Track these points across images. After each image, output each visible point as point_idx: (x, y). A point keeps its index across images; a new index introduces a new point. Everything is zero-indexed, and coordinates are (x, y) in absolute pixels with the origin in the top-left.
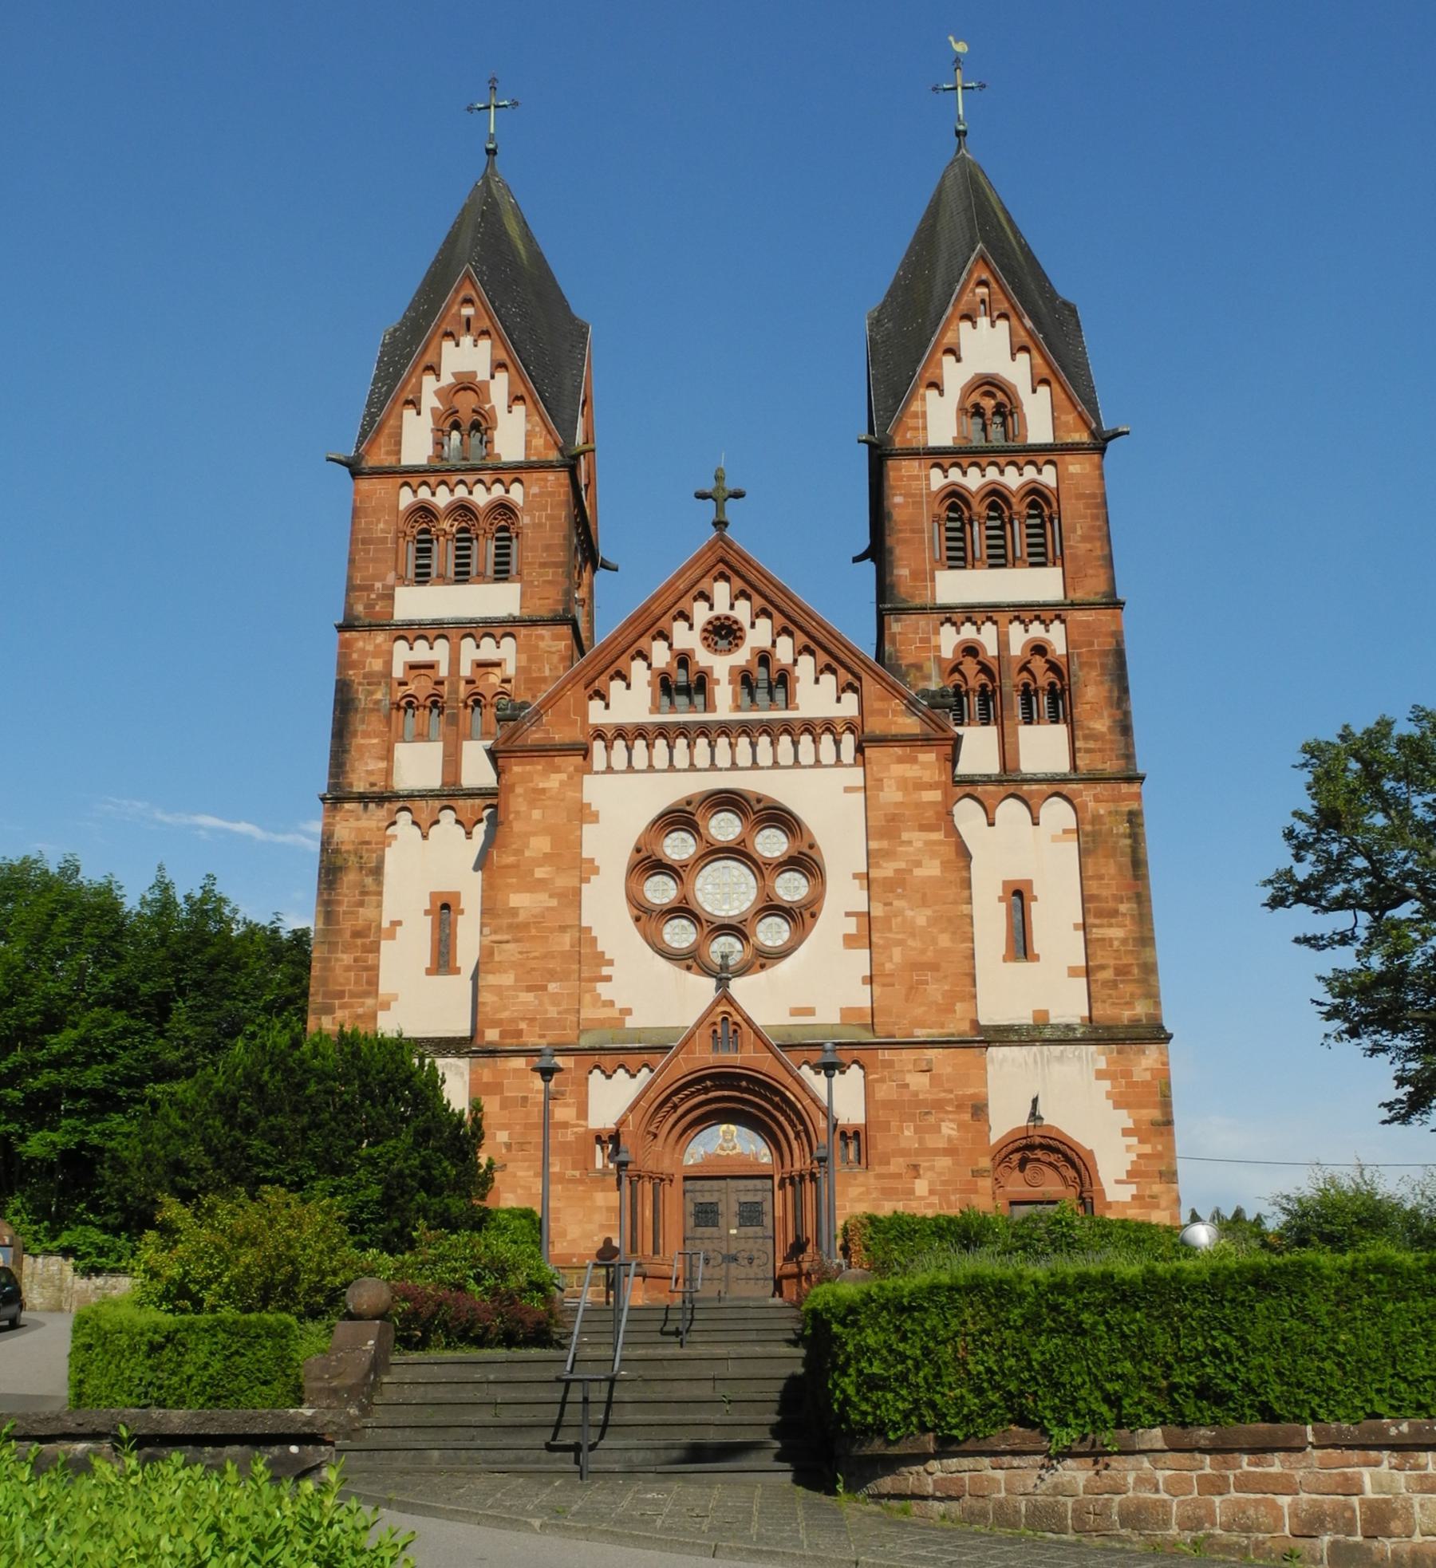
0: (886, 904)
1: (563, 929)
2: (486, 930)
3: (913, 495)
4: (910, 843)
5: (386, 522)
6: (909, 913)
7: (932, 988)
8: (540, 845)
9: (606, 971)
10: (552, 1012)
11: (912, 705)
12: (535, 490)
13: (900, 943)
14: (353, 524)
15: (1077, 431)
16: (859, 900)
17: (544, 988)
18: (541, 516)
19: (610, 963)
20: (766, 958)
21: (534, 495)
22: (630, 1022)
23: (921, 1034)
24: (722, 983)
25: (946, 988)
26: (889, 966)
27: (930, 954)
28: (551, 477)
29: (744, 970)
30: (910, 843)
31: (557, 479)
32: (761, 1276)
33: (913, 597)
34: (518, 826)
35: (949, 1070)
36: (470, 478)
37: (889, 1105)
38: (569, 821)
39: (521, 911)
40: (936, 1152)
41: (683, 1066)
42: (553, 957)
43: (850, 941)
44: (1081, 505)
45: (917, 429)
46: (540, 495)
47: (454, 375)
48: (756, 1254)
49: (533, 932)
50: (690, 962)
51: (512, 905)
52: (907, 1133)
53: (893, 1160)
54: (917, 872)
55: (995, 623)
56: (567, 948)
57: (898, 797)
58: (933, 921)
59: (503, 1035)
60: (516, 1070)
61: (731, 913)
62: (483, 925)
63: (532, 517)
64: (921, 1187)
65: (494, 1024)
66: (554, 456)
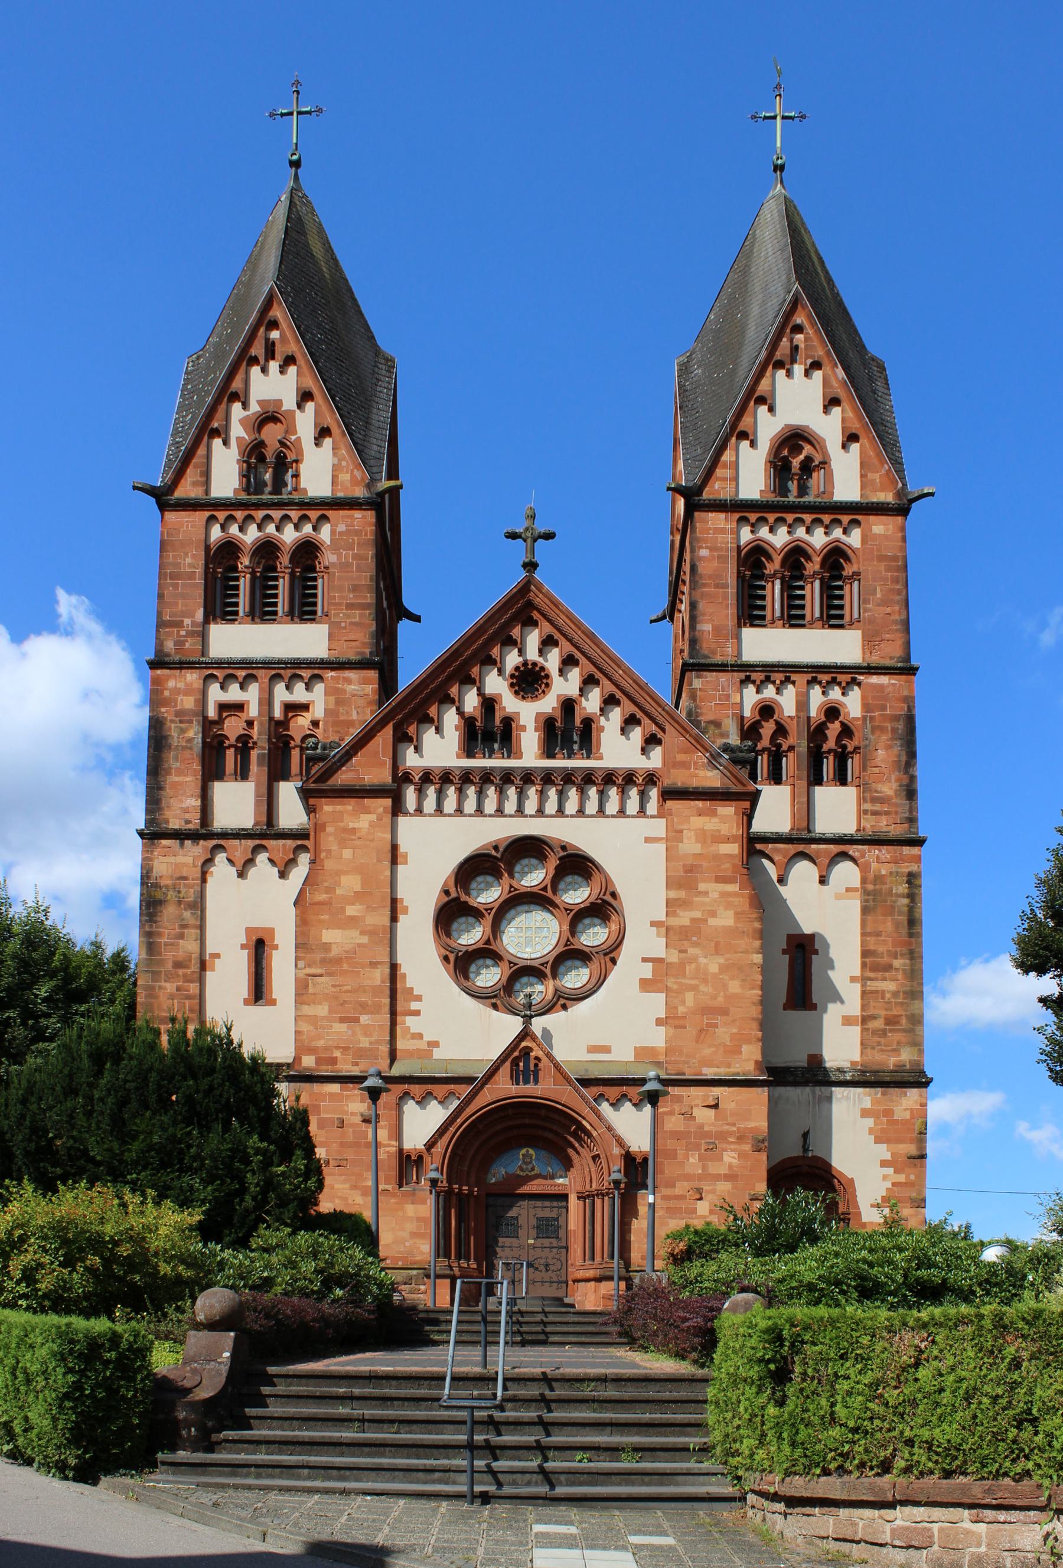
0: (680, 951)
1: (373, 965)
2: (301, 964)
3: (721, 549)
4: (706, 893)
5: (193, 556)
6: (702, 960)
7: (720, 1030)
8: (351, 883)
9: (414, 1006)
10: (365, 1042)
11: (713, 759)
12: (341, 528)
13: (694, 988)
14: (161, 557)
15: (882, 490)
16: (658, 947)
17: (357, 1020)
18: (348, 555)
19: (419, 998)
20: (563, 1000)
21: (340, 533)
22: (438, 1054)
23: (709, 1073)
24: (527, 1020)
25: (735, 1031)
26: (681, 1010)
27: (721, 999)
28: (358, 514)
29: (548, 1009)
30: (706, 893)
31: (364, 517)
32: (555, 1279)
33: (714, 653)
34: (329, 865)
35: (733, 1105)
36: (277, 514)
37: (677, 1136)
38: (379, 861)
39: (334, 947)
40: (717, 1177)
41: (487, 1096)
42: (364, 991)
43: (646, 985)
44: (882, 566)
45: (724, 479)
46: (348, 532)
47: (260, 402)
48: (550, 1261)
49: (345, 967)
50: (494, 1001)
51: (324, 940)
52: (691, 1160)
53: (678, 1184)
54: (712, 922)
55: (793, 683)
56: (378, 983)
57: (697, 848)
58: (724, 969)
59: (318, 1061)
60: (331, 1095)
61: (533, 956)
62: (297, 959)
63: (339, 557)
64: (703, 1208)
65: (311, 1051)
66: (360, 492)
